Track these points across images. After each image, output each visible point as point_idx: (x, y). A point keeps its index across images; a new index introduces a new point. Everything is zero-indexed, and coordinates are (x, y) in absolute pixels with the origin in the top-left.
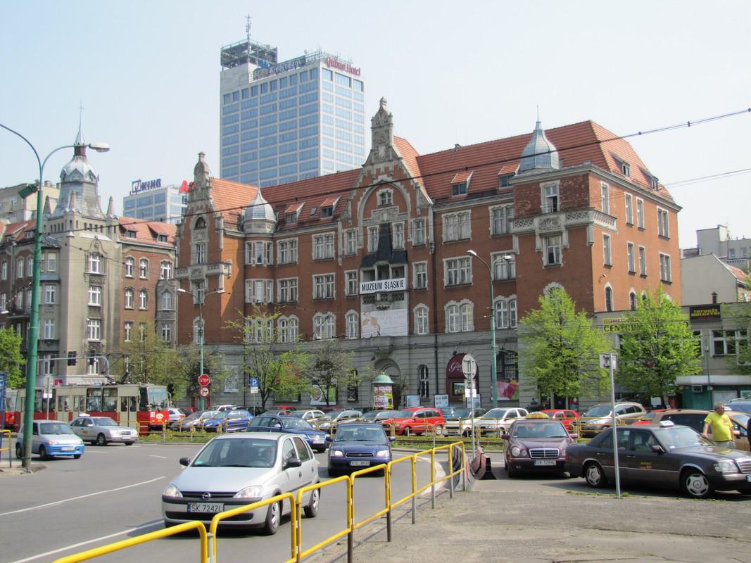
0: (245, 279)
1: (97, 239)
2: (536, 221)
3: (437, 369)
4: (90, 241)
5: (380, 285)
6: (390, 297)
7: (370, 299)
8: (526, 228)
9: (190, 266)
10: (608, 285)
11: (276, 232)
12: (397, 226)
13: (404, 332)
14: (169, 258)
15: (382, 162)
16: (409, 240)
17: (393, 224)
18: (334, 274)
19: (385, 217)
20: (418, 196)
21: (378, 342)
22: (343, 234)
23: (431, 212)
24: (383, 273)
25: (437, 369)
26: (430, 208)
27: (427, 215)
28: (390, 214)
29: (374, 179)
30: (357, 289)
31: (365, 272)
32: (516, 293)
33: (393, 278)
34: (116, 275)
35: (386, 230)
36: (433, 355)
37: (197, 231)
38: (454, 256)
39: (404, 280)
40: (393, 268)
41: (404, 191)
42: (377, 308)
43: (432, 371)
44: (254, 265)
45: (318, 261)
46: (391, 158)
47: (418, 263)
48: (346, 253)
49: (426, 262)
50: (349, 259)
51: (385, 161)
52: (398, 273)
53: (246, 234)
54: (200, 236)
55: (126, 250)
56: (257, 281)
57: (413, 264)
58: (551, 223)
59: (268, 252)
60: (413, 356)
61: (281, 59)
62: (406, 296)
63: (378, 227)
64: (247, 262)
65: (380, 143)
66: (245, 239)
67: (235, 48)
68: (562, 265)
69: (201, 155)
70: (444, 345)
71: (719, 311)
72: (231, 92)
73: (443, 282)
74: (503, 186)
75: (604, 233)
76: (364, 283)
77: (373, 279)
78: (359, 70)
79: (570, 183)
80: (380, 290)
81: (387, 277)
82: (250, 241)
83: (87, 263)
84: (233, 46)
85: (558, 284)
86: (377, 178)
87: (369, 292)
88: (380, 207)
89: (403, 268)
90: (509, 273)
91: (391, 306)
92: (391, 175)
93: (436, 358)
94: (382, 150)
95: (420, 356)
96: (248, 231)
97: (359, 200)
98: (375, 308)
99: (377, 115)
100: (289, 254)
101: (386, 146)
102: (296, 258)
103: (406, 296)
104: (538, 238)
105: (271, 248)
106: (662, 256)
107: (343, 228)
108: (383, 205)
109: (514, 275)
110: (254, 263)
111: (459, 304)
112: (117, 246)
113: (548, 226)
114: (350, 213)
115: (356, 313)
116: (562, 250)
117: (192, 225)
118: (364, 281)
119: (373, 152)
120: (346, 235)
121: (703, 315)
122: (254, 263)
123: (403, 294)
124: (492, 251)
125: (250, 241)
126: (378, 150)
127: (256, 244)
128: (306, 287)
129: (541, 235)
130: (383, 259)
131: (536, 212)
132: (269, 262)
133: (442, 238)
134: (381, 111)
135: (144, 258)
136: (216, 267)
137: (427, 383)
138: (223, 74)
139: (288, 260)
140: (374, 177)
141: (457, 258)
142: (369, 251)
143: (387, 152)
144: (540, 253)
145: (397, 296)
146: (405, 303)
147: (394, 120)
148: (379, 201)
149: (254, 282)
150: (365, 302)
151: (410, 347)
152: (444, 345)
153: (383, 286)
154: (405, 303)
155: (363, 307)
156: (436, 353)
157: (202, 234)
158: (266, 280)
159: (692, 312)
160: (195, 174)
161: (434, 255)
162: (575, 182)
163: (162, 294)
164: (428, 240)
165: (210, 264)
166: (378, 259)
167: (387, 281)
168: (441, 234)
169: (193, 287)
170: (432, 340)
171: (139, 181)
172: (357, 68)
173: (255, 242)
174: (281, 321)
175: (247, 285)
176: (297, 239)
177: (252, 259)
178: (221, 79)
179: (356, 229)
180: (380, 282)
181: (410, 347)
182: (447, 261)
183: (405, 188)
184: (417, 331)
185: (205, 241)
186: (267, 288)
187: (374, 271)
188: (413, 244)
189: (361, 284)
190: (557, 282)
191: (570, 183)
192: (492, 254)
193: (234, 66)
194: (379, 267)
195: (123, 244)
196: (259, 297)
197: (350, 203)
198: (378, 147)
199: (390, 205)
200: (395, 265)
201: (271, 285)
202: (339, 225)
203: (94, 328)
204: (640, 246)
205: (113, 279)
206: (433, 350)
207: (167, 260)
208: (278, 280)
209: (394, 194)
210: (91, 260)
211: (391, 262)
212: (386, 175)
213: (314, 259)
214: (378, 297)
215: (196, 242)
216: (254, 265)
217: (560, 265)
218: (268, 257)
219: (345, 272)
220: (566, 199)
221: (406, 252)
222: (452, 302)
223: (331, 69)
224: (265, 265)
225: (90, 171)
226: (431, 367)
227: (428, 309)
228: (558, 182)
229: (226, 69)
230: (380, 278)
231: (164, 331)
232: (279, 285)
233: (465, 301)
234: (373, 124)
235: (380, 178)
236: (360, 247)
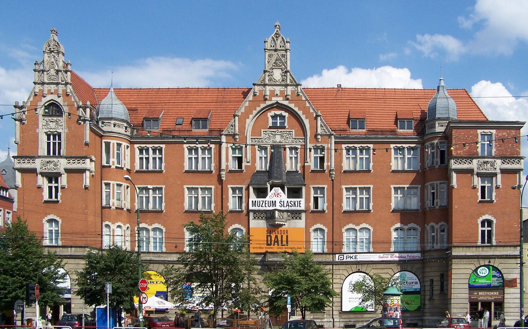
19: (278, 139)
29: (266, 100)
31: (254, 189)
35: (278, 149)
39: (303, 200)
41: (303, 117)
42: (270, 225)
57: (311, 186)
62: (303, 215)
87: (261, 208)
88: (270, 128)
89: (301, 188)
97: (248, 118)
108: (274, 127)
124: (393, 184)
130: (277, 178)
140: (268, 97)
177: (111, 160)
183: (303, 114)
199: (284, 128)
212: (281, 98)
216: (113, 167)
222: (351, 226)
235: (274, 100)
236: (248, 164)
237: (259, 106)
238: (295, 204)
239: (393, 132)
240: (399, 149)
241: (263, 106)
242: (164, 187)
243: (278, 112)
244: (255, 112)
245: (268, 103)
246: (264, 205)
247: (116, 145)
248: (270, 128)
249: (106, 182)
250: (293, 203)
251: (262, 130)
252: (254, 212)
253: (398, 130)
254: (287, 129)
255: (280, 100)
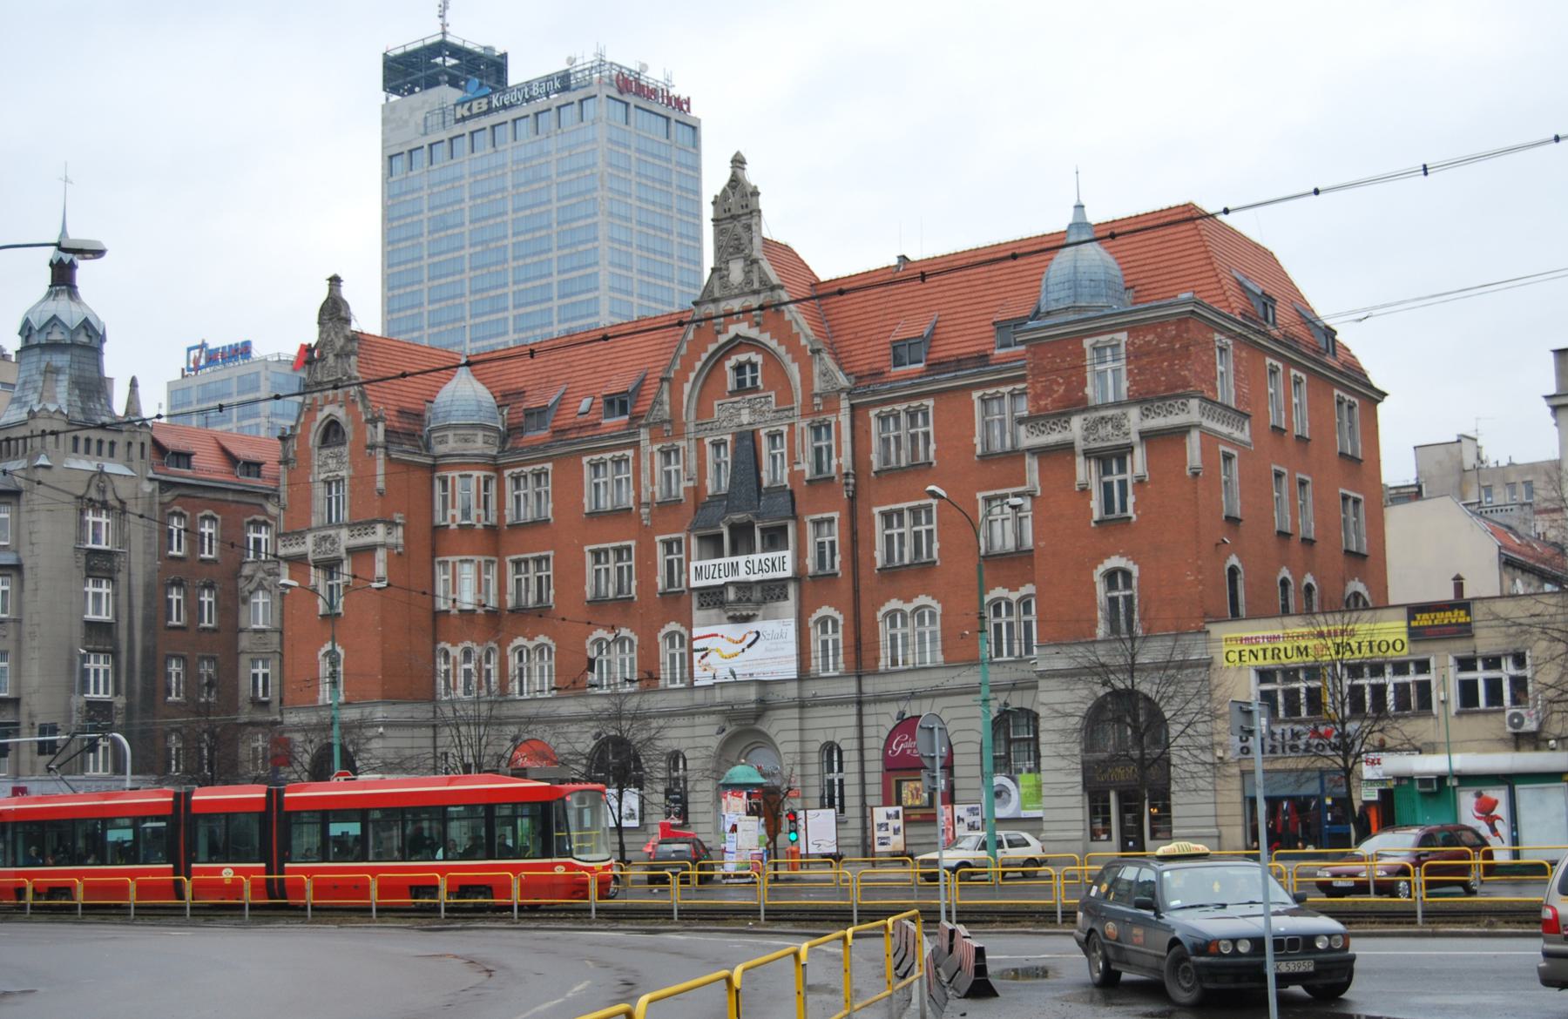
0: (433, 556)
1: (101, 473)
2: (1077, 423)
3: (861, 750)
4: (87, 477)
5: (735, 568)
6: (757, 594)
7: (712, 597)
8: (1054, 438)
9: (310, 530)
10: (1234, 560)
11: (502, 451)
12: (773, 437)
13: (790, 670)
14: (265, 512)
15: (736, 296)
16: (797, 468)
17: (762, 433)
18: (632, 543)
19: (745, 417)
20: (816, 370)
21: (731, 694)
22: (652, 454)
23: (845, 404)
24: (742, 540)
25: (861, 750)
26: (843, 395)
27: (837, 410)
28: (753, 412)
29: (719, 332)
30: (684, 577)
31: (701, 538)
32: (1032, 581)
33: (764, 550)
34: (145, 553)
35: (747, 444)
36: (853, 720)
37: (326, 452)
38: (897, 502)
39: (788, 555)
40: (763, 530)
41: (787, 359)
43: (851, 757)
44: (453, 526)
45: (596, 515)
46: (756, 286)
47: (818, 516)
48: (658, 498)
49: (836, 515)
50: (668, 506)
51: (742, 294)
52: (775, 538)
53: (435, 458)
54: (332, 463)
55: (168, 497)
56: (461, 561)
57: (807, 519)
58: (1109, 427)
59: (486, 497)
60: (809, 724)
61: (515, 77)
62: (792, 590)
63: (729, 438)
64: (439, 520)
65: (731, 254)
66: (433, 468)
67: (415, 53)
68: (1134, 518)
69: (335, 281)
70: (879, 699)
71: (1468, 614)
72: (405, 149)
73: (873, 559)
74: (1002, 346)
75: (1222, 448)
76: (699, 564)
77: (720, 554)
78: (688, 102)
79: (1149, 337)
80: (735, 578)
81: (752, 550)
82: (444, 473)
83: (82, 524)
84: (409, 48)
85: (1124, 560)
86: (726, 331)
87: (711, 582)
88: (733, 394)
89: (784, 529)
90: (1019, 538)
91: (760, 613)
92: (758, 324)
93: (860, 726)
94: (736, 271)
95: (828, 723)
96: (440, 449)
98: (724, 617)
99: (724, 191)
100: (532, 499)
101: (745, 259)
102: (548, 511)
103: (792, 590)
104: (1080, 460)
105: (493, 486)
106: (1345, 498)
107: (653, 440)
108: (741, 388)
109: (1029, 542)
110: (454, 521)
111: (908, 608)
112: (148, 487)
113: (1102, 432)
114: (667, 408)
115: (683, 630)
116: (1134, 485)
117: (314, 439)
118: (700, 559)
119: (716, 275)
120: (657, 457)
121: (1436, 622)
122: (454, 521)
123: (785, 587)
124: (980, 490)
125: (444, 473)
126: (727, 269)
127: (457, 479)
128: (571, 575)
129: (1088, 454)
131: (1076, 404)
132: (486, 519)
133: (870, 463)
134: (735, 182)
135: (208, 512)
136: (369, 531)
137: (841, 781)
138: (387, 109)
139: (528, 514)
141: (905, 505)
142: (710, 492)
143: (747, 273)
144: (1085, 490)
145: (772, 590)
146: (789, 606)
147: (764, 203)
148: (731, 383)
149: (454, 563)
150: (701, 606)
151: (802, 704)
152: (879, 699)
153: (742, 569)
154: (789, 606)
155: (698, 615)
156: (860, 715)
157: (337, 457)
158: (482, 559)
159: (1411, 617)
160: (320, 323)
161: (852, 499)
162: (1160, 337)
163: (251, 593)
164: (839, 466)
165: (355, 524)
166: (729, 510)
167: (751, 557)
168: (869, 451)
169: (317, 578)
170: (850, 688)
171: (202, 346)
172: (684, 97)
173: (456, 474)
174: (515, 649)
175: (439, 570)
176: (549, 466)
177: (450, 512)
178: (385, 121)
179: (681, 443)
180: (734, 559)
181: (802, 704)
182: (883, 514)
184: (816, 664)
185: (343, 473)
186: (484, 577)
187: (721, 536)
188: (807, 476)
189: (693, 565)
190: (1122, 555)
191: (1149, 337)
192: (979, 496)
193: (411, 92)
194: (734, 528)
195: (162, 482)
196: (467, 598)
197: (666, 385)
198: (727, 262)
199: (755, 389)
200: (768, 524)
201: (494, 570)
202: (644, 435)
203: (97, 672)
204: (1299, 476)
205: (139, 565)
206: (853, 710)
207: (261, 518)
208: (508, 559)
209: (765, 364)
210: (90, 518)
211: (758, 516)
212: (746, 324)
213: (587, 510)
214: (731, 595)
215: (323, 476)
216: (453, 526)
217: (1130, 518)
218: (486, 507)
219: (658, 539)
220: (1138, 374)
221: (792, 493)
222: (894, 604)
223: (626, 98)
224: (479, 526)
225: (86, 320)
226: (849, 745)
227: (840, 618)
228: (1123, 337)
229: (394, 98)
230: (734, 552)
231: (255, 676)
232: (510, 569)
233: (922, 600)
234: (716, 211)
235: (733, 330)
236: (691, 484)
237: (706, 351)
238: (773, 564)
239: (982, 359)
240: (993, 397)
241: (712, 348)
242: (551, 553)
243: (743, 357)
244: (698, 365)
245: (723, 339)
246: (716, 575)
247: (457, 479)
248: (733, 394)
249: (440, 559)
250: (770, 564)
251: (716, 403)
252: (704, 592)
253: (996, 352)
254: (763, 391)
255: (742, 329)
